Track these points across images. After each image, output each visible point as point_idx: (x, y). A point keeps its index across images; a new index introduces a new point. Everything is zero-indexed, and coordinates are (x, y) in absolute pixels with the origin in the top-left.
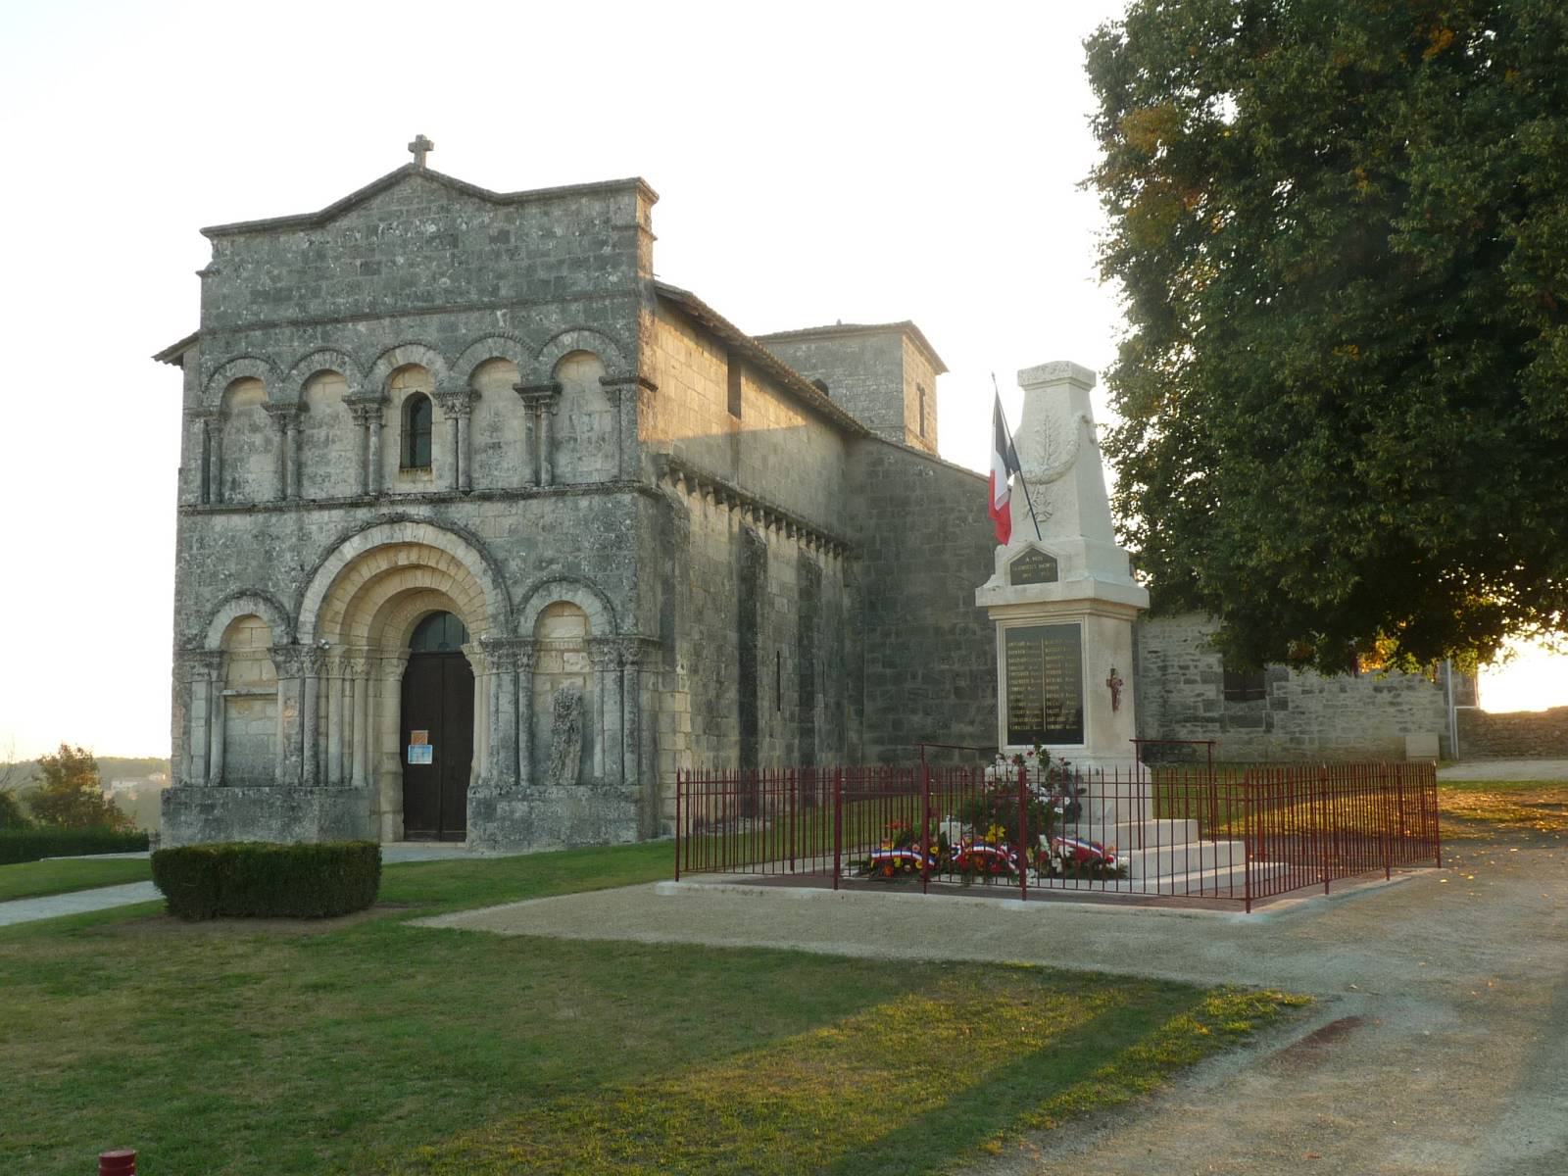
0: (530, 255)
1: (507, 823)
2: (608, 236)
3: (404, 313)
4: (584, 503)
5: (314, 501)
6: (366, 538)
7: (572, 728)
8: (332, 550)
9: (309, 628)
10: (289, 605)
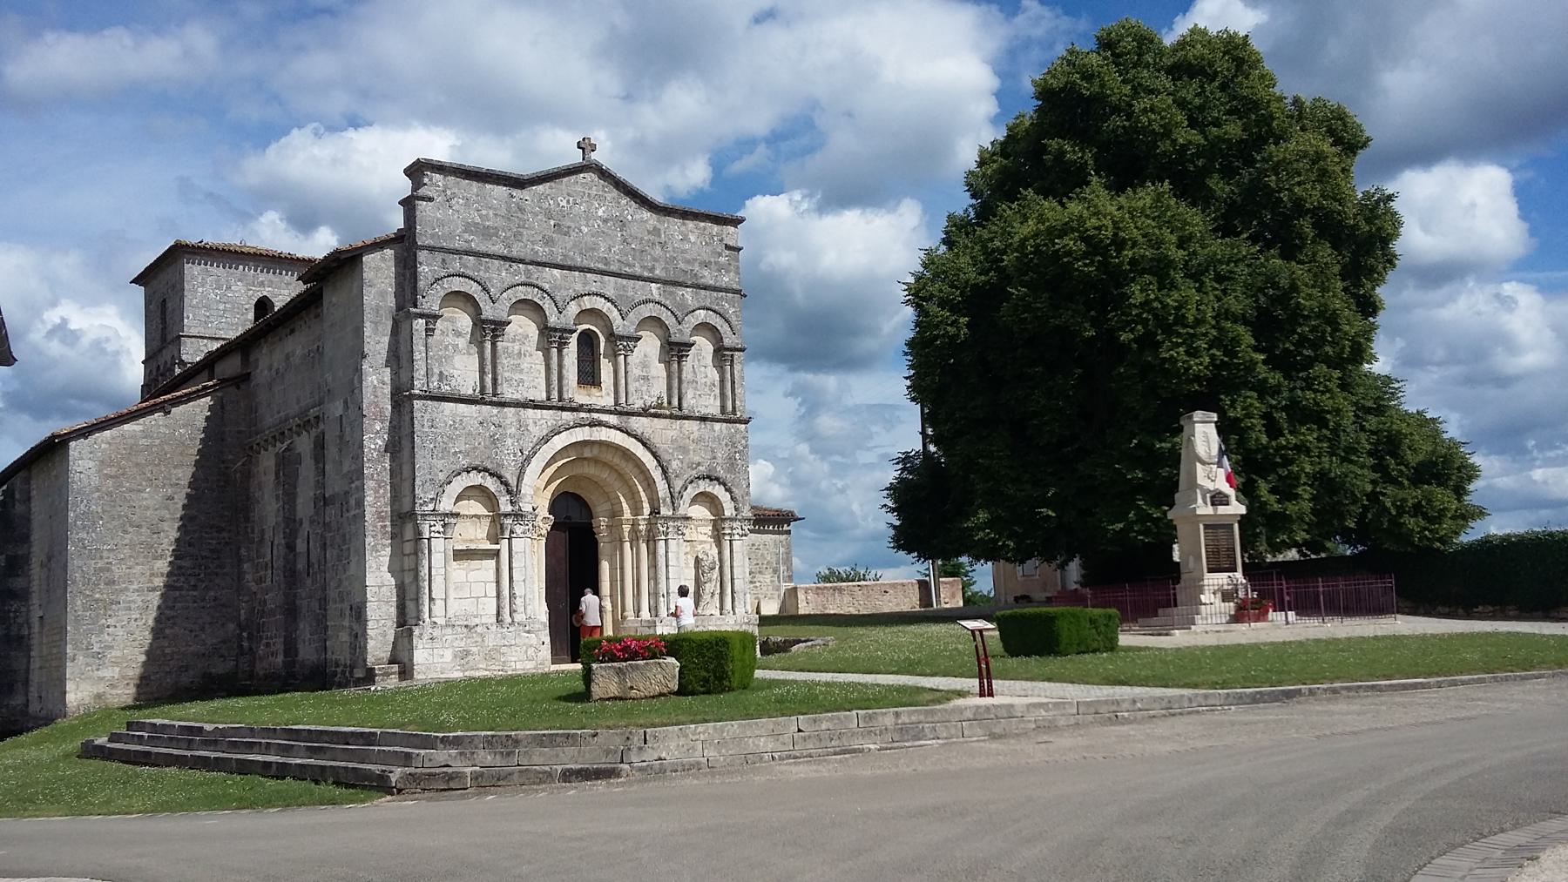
3: (590, 271)
8: (546, 440)
10: (513, 482)
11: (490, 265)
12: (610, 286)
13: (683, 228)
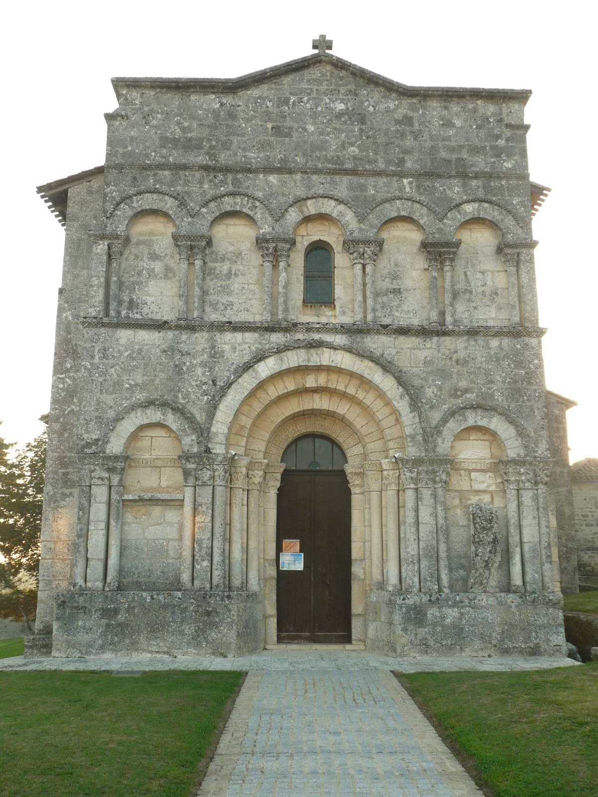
0: (432, 138)
1: (439, 629)
2: (502, 132)
3: (317, 171)
4: (494, 343)
5: (230, 323)
6: (281, 360)
7: (495, 541)
8: (247, 367)
9: (221, 438)
10: (200, 416)
11: (190, 178)
12: (343, 186)
13: (445, 112)
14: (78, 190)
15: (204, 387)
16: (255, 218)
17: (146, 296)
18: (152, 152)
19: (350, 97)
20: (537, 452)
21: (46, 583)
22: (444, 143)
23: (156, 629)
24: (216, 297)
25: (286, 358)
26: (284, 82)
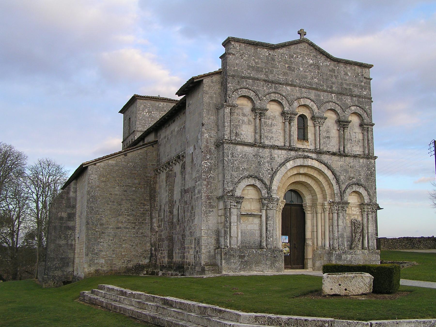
2: (363, 80)
3: (304, 87)
4: (361, 161)
5: (278, 146)
6: (295, 162)
8: (283, 164)
10: (268, 183)
11: (259, 84)
12: (313, 94)
14: (208, 80)
15: (269, 171)
16: (283, 103)
17: (242, 131)
18: (244, 71)
19: (314, 58)
20: (373, 201)
21: (205, 246)
22: (345, 81)
23: (258, 263)
24: (267, 134)
25: (296, 161)
26: (291, 48)
